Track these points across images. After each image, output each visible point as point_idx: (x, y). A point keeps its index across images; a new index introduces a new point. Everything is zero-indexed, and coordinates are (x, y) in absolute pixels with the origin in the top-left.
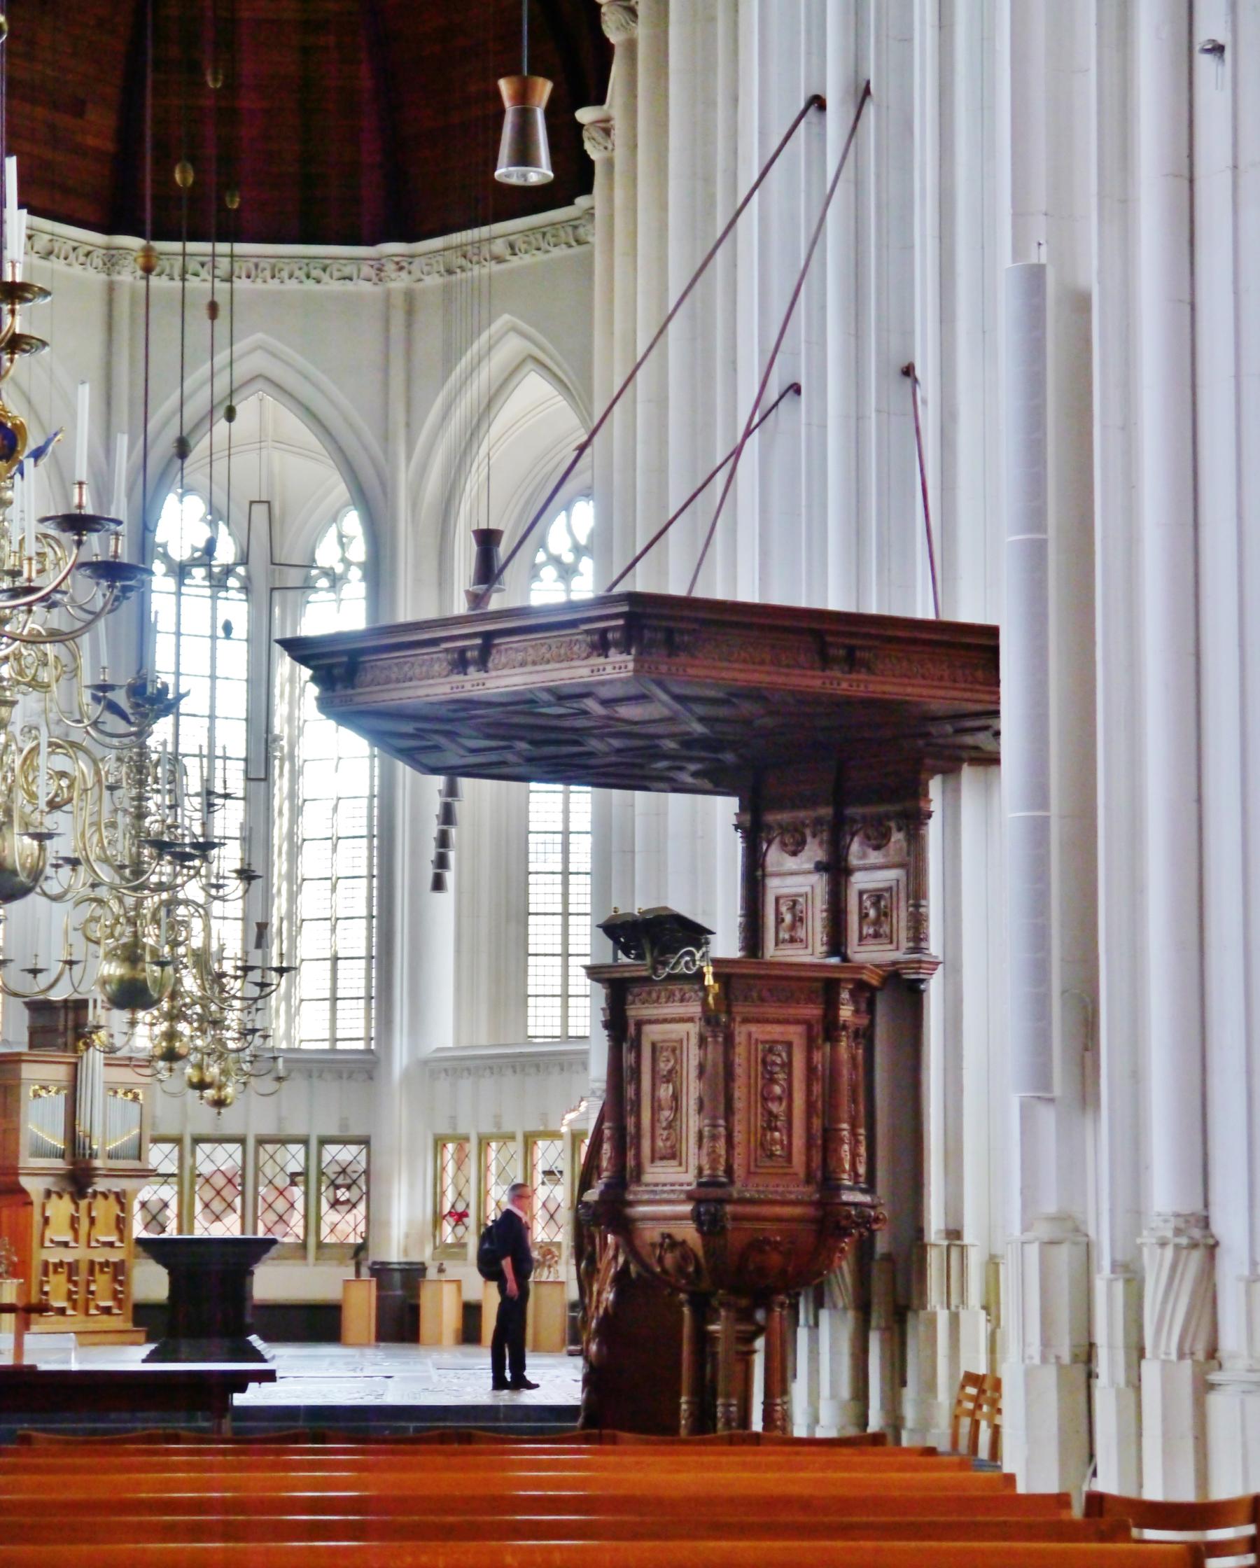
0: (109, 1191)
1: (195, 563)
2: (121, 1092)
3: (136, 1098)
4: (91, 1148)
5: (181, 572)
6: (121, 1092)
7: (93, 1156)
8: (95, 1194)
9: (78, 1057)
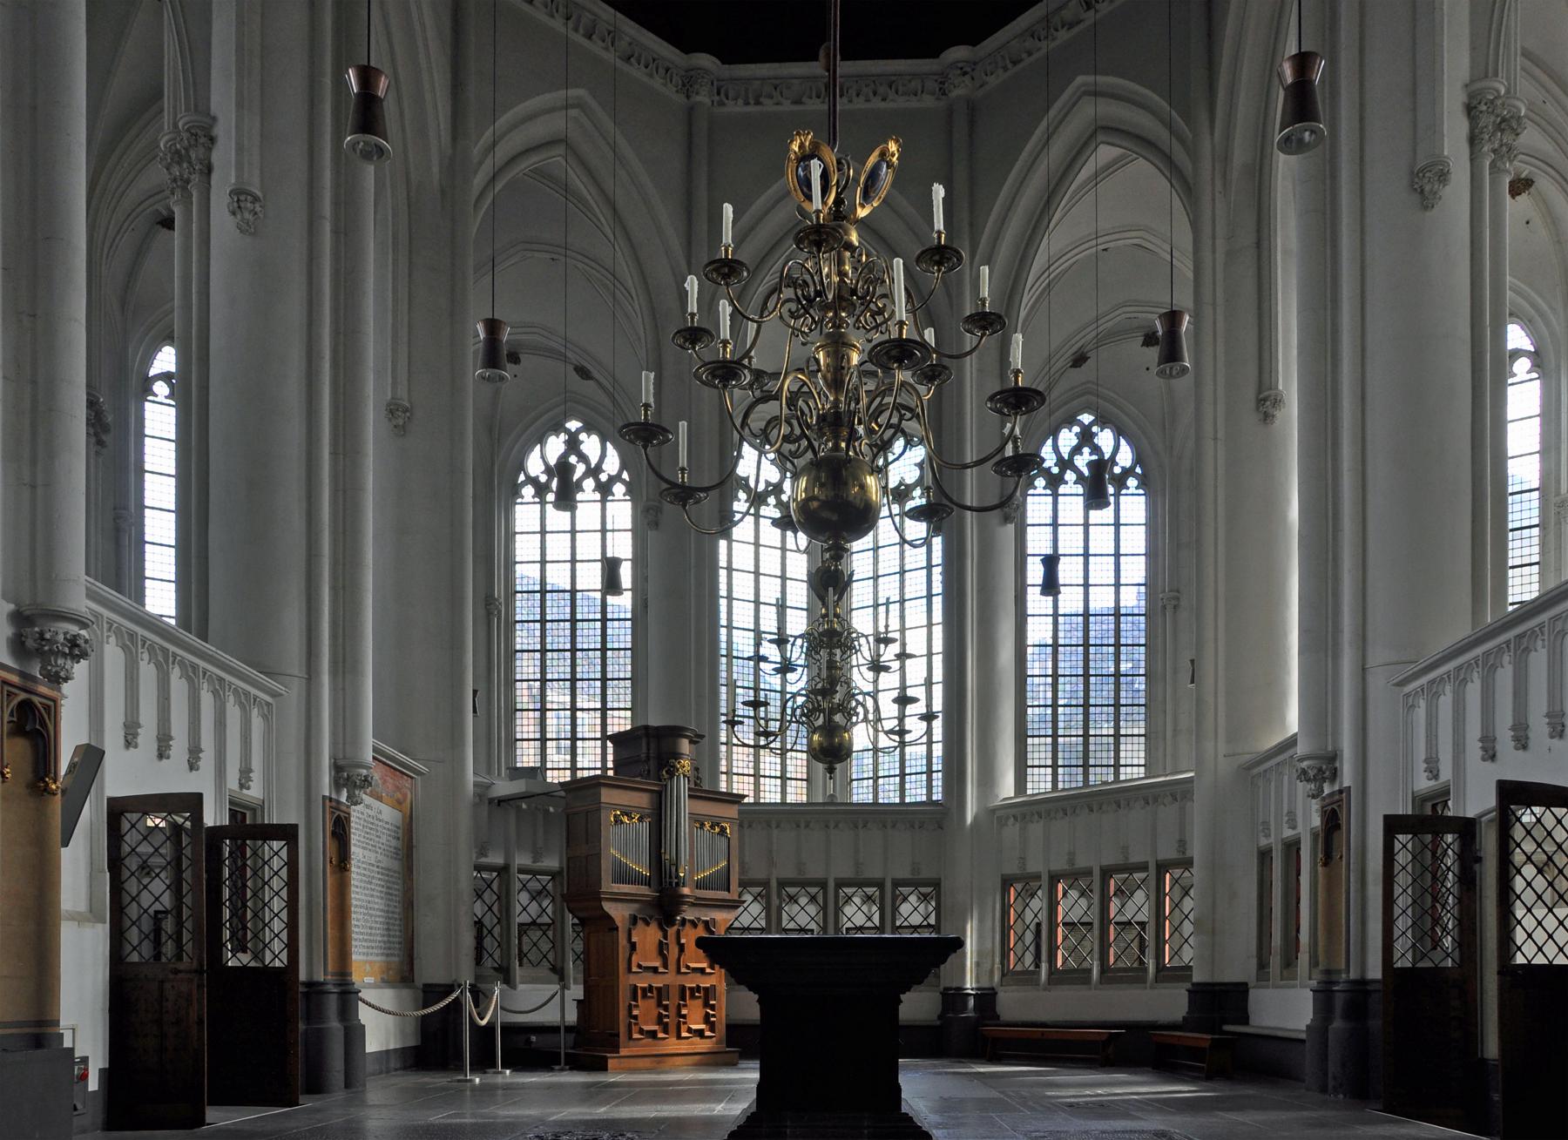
0: (699, 919)
1: (766, 494)
2: (707, 826)
3: (723, 830)
4: (677, 876)
5: (757, 499)
6: (707, 826)
7: (680, 883)
8: (684, 921)
9: (662, 786)
